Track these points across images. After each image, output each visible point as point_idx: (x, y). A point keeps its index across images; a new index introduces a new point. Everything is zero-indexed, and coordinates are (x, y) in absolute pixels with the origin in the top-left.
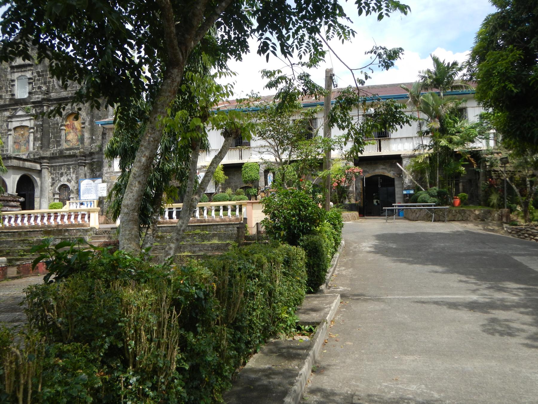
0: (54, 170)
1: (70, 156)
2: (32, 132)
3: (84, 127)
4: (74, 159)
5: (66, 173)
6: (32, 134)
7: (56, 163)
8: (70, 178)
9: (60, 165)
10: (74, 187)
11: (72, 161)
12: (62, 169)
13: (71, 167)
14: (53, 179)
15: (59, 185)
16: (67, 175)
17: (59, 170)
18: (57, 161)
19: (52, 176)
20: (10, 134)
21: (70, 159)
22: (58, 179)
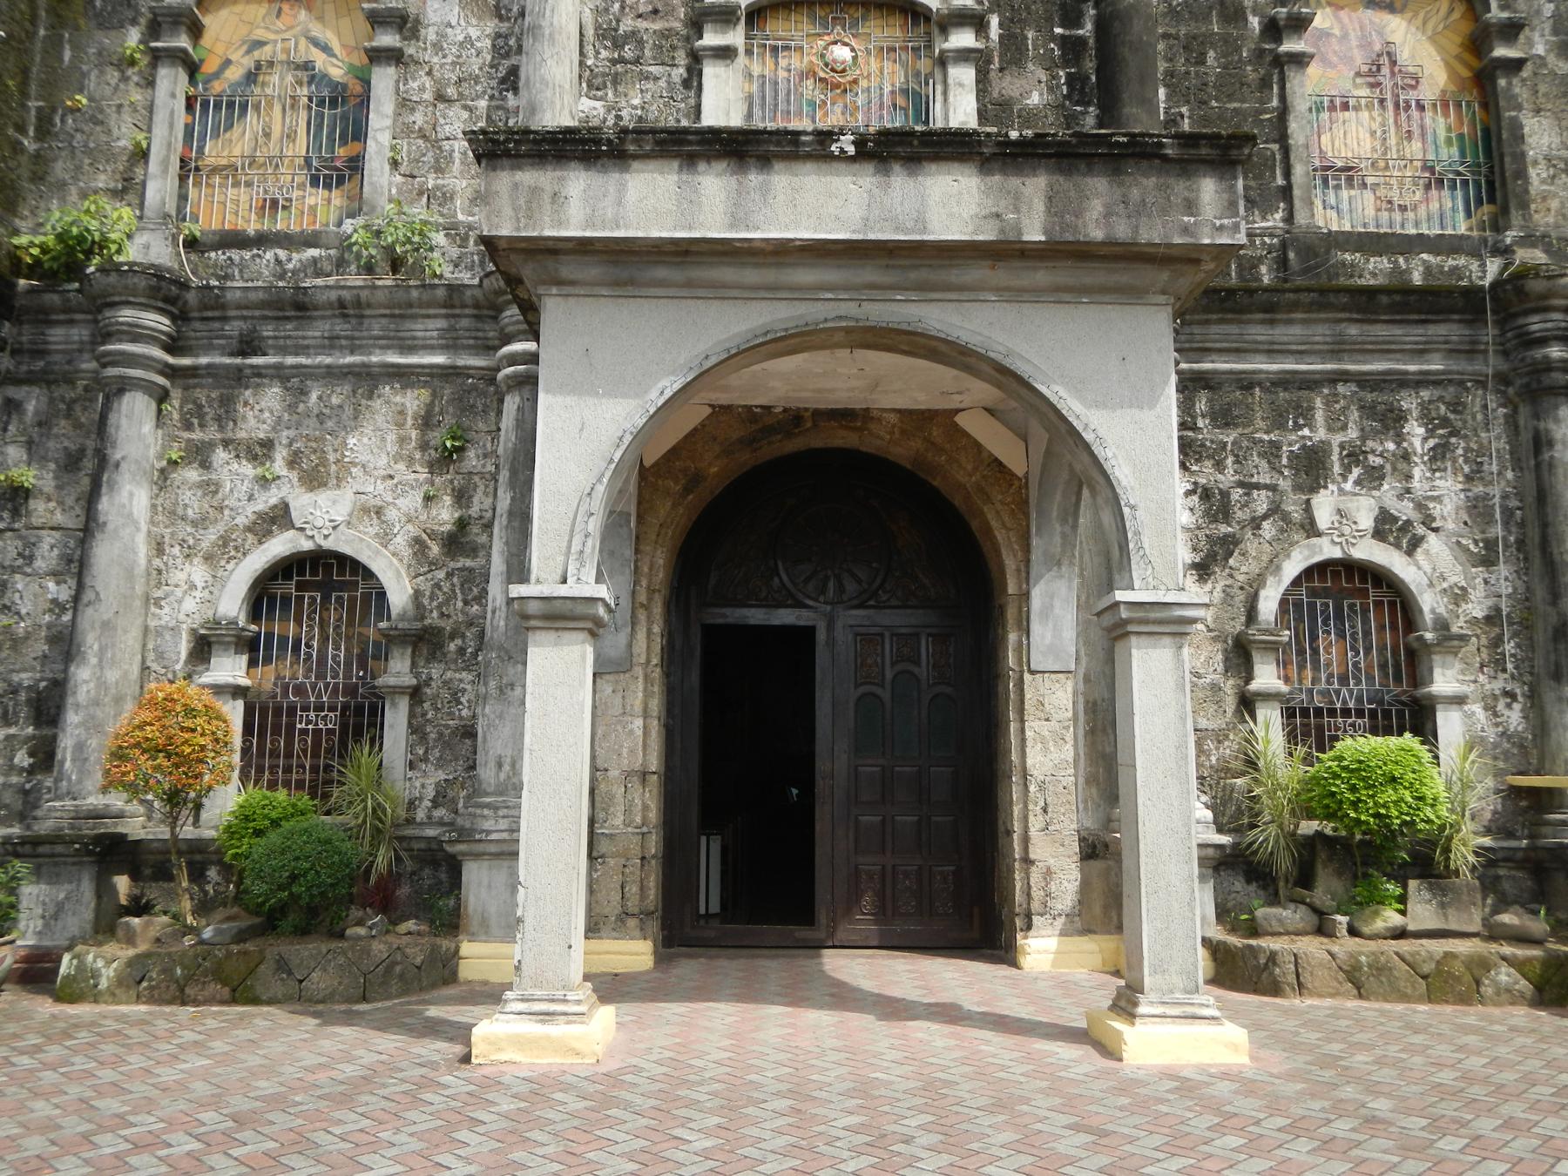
0: (1223, 418)
1: (1404, 303)
2: (964, 55)
3: (1516, 65)
4: (1449, 331)
5: (1354, 456)
6: (964, 75)
7: (1238, 352)
8: (1405, 510)
9: (1285, 381)
10: (1459, 596)
11: (1420, 353)
12: (1305, 414)
13: (1409, 402)
14: (1213, 503)
15: (1293, 567)
16: (1373, 477)
17: (1278, 423)
18: (1258, 332)
19: (1206, 473)
20: (725, 53)
21: (1413, 334)
22: (1275, 510)
